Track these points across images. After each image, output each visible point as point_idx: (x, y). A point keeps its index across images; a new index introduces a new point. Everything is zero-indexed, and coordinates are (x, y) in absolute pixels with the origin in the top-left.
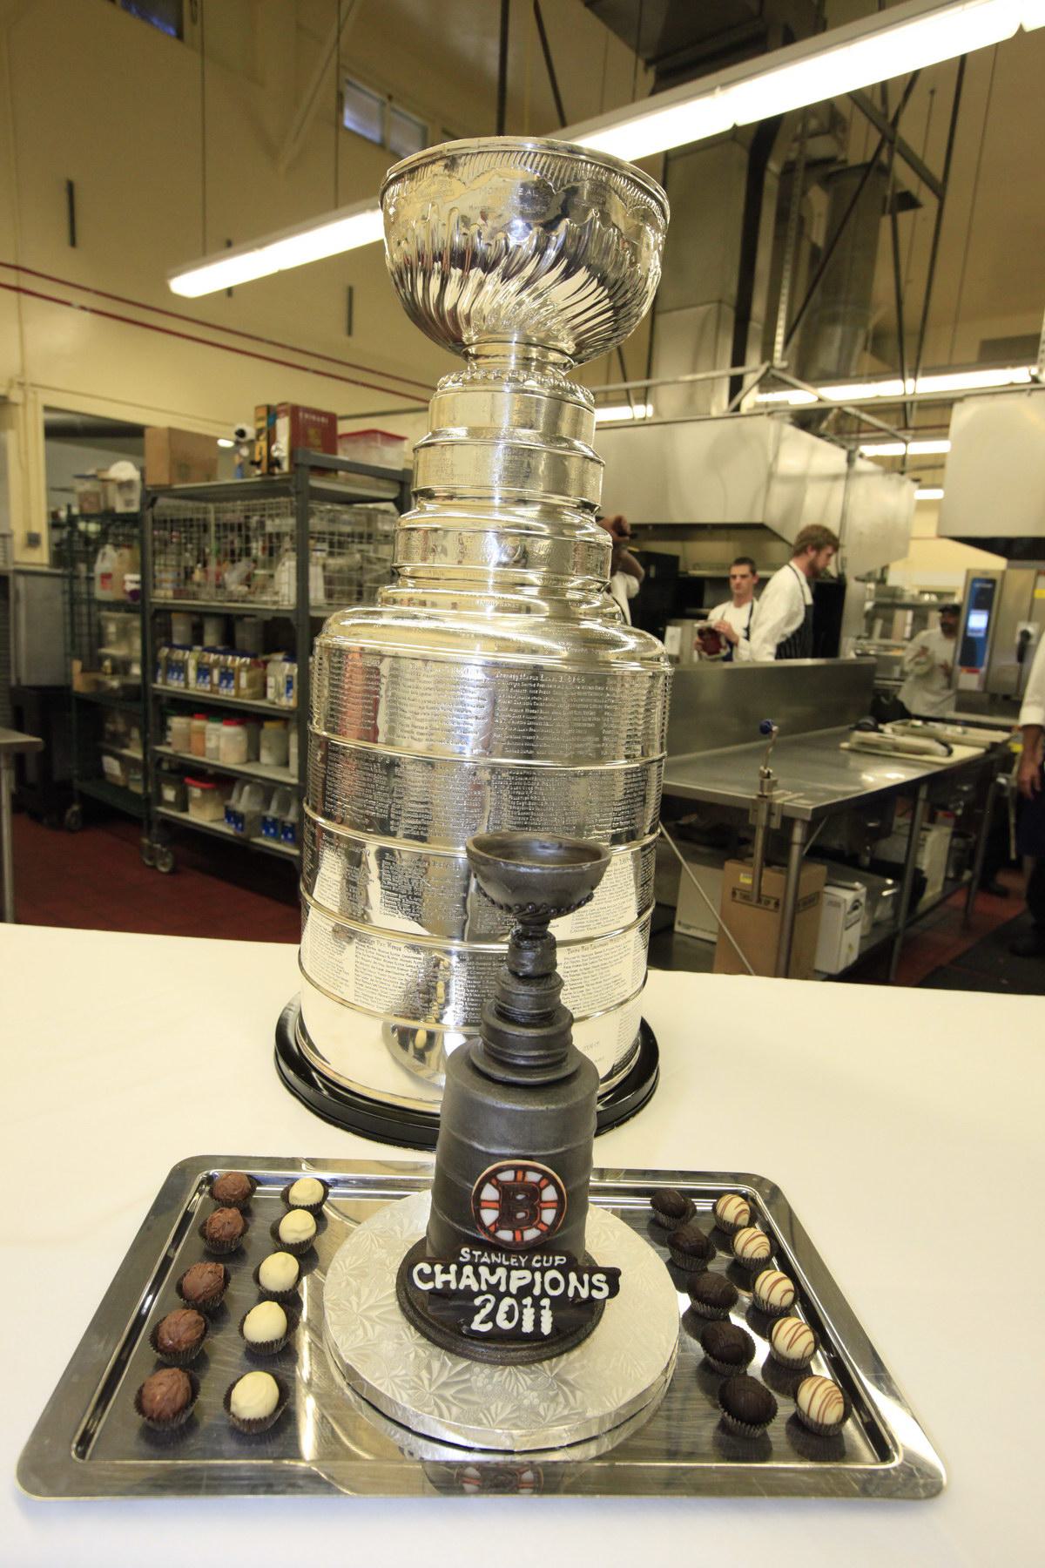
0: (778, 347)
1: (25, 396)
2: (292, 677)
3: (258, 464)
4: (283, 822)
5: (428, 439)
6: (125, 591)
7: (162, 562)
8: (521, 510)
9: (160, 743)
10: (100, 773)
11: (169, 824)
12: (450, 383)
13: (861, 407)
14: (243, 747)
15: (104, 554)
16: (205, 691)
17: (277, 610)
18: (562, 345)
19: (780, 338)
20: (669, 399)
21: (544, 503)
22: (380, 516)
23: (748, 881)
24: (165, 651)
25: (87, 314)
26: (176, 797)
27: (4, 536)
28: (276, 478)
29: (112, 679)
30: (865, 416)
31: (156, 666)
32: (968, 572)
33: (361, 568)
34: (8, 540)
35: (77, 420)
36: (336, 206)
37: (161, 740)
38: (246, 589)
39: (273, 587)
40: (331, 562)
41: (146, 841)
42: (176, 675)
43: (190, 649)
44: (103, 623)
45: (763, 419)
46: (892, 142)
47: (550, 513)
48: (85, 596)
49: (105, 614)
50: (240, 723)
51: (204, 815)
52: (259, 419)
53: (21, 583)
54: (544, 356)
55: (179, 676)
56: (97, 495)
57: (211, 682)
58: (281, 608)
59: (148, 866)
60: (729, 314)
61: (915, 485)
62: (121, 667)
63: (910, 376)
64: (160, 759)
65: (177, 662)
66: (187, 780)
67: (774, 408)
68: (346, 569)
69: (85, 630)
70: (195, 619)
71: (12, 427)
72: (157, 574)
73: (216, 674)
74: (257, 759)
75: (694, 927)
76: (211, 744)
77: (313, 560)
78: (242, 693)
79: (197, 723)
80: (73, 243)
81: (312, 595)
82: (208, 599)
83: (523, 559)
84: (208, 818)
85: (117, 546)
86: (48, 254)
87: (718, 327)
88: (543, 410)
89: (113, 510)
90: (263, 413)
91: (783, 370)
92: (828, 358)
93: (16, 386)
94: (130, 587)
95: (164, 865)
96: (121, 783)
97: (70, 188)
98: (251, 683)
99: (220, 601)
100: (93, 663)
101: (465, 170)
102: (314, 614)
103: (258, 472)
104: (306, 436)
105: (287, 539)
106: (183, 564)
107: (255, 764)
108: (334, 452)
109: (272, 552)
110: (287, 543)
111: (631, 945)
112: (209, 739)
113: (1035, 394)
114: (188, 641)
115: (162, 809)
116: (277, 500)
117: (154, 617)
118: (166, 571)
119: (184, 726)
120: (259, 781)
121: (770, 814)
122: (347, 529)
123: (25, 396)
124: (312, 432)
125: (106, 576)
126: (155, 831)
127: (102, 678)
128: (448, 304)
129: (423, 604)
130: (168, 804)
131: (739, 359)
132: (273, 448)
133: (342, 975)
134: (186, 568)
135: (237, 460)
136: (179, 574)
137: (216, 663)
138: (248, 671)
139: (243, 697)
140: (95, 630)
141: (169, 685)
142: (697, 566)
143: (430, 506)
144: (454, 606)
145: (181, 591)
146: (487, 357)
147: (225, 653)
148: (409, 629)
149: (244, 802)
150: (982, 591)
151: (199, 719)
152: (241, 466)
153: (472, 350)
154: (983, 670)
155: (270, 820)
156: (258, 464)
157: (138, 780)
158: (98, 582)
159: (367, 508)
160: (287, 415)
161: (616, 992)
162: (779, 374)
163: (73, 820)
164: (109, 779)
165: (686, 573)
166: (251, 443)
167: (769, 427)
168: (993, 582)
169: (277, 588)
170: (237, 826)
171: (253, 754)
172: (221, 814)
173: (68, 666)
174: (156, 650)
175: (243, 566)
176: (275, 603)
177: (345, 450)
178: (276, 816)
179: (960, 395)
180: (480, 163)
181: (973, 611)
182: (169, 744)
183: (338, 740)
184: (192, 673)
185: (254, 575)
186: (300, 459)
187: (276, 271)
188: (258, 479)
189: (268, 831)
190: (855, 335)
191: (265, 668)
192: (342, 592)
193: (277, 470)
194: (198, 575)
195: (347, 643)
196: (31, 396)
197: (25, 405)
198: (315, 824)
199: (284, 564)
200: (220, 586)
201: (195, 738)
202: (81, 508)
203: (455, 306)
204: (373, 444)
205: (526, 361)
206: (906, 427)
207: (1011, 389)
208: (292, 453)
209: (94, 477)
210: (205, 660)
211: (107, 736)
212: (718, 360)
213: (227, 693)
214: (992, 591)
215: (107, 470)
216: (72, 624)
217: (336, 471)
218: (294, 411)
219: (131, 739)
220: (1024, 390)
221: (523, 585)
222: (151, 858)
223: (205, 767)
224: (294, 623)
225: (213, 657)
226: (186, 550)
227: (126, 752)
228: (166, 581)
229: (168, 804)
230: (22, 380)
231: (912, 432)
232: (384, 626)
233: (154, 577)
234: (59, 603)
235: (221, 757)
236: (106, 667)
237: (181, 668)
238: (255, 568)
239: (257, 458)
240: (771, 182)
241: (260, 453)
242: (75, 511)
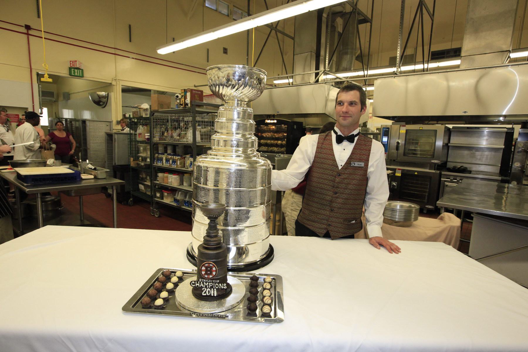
0: (327, 65)
1: (116, 83)
2: (192, 162)
3: (182, 105)
4: (190, 202)
5: (217, 120)
6: (145, 138)
7: (156, 130)
8: (237, 135)
9: (155, 181)
10: (138, 189)
11: (158, 203)
12: (221, 109)
13: (352, 81)
14: (179, 181)
15: (139, 128)
16: (169, 166)
17: (188, 143)
18: (246, 100)
19: (327, 63)
20: (298, 79)
21: (242, 134)
22: (215, 117)
24: (157, 155)
25: (134, 60)
26: (160, 195)
27: (110, 122)
28: (187, 108)
29: (142, 163)
30: (353, 82)
31: (154, 159)
32: (381, 125)
33: (210, 131)
34: (111, 123)
35: (130, 88)
36: (203, 31)
37: (156, 180)
38: (179, 137)
39: (187, 137)
40: (202, 130)
41: (151, 208)
42: (160, 161)
43: (164, 155)
44: (139, 147)
45: (324, 84)
47: (244, 136)
48: (134, 140)
49: (140, 144)
50: (177, 175)
51: (168, 200)
52: (182, 93)
53: (116, 136)
54: (241, 102)
55: (161, 162)
56: (138, 112)
57: (170, 163)
58: (188, 143)
59: (153, 215)
61: (369, 100)
62: (144, 159)
63: (365, 70)
64: (156, 184)
65: (160, 158)
66: (163, 191)
67: (327, 82)
68: (206, 132)
69: (134, 149)
70: (165, 145)
71: (113, 92)
72: (154, 134)
73: (171, 161)
74: (183, 184)
76: (170, 181)
77: (197, 130)
78: (178, 166)
79: (166, 175)
80: (130, 41)
81: (197, 140)
82: (168, 141)
83: (238, 146)
84: (169, 202)
85: (143, 125)
86: (124, 44)
87: (311, 59)
88: (241, 115)
89: (142, 116)
90: (184, 92)
91: (328, 71)
92: (344, 64)
93: (114, 80)
94: (147, 137)
95: (157, 215)
96: (144, 192)
97: (130, 26)
98: (181, 163)
99: (171, 141)
100: (136, 158)
101: (222, 70)
102: (197, 144)
103: (182, 107)
104: (195, 97)
105: (190, 123)
106: (161, 131)
107: (182, 186)
108: (203, 101)
109: (187, 128)
110: (190, 125)
111: (264, 228)
112: (169, 179)
113: (395, 77)
114: (163, 151)
115: (156, 199)
116: (187, 114)
117: (153, 145)
118: (157, 133)
119: (162, 176)
120: (183, 191)
122: (207, 120)
123: (116, 83)
124: (196, 96)
125: (140, 134)
126: (154, 205)
127: (140, 163)
128: (220, 92)
129: (217, 155)
130: (158, 198)
131: (317, 68)
132: (186, 101)
133: (201, 235)
134: (162, 132)
135: (176, 103)
136: (160, 134)
137: (171, 158)
138: (179, 160)
139: (178, 168)
140: (137, 149)
141: (158, 164)
142: (308, 125)
143: (218, 134)
144: (224, 156)
145: (161, 138)
146: (229, 103)
147: (173, 155)
148: (213, 161)
149: (179, 197)
150: (386, 131)
151: (166, 173)
152: (177, 105)
153: (227, 101)
155: (186, 201)
156: (182, 105)
157: (149, 191)
158: (138, 135)
159: (213, 115)
160: (189, 91)
161: (262, 237)
162: (327, 72)
163: (131, 203)
164: (140, 190)
165: (305, 127)
166: (180, 99)
167: (326, 86)
168: (388, 128)
169: (187, 137)
170: (177, 203)
171: (182, 183)
172: (173, 200)
173: (129, 160)
174: (154, 155)
175: (178, 131)
176: (187, 141)
177: (205, 100)
178: (188, 200)
180: (225, 69)
181: (383, 137)
182: (158, 181)
183: (199, 185)
184: (164, 161)
185: (181, 133)
186: (193, 104)
187: (186, 47)
188: (182, 108)
189: (186, 204)
190: (352, 57)
191: (185, 159)
192: (205, 138)
193: (187, 106)
194: (166, 134)
195: (201, 164)
196: (118, 83)
197: (116, 85)
198: (194, 203)
199: (189, 131)
200: (172, 137)
201: (165, 179)
202: (133, 115)
203: (222, 93)
204: (213, 98)
205: (238, 104)
206: (366, 85)
208: (191, 102)
209: (137, 107)
210: (168, 157)
211: (140, 179)
212: (312, 68)
213: (174, 166)
215: (141, 106)
216: (130, 149)
217: (203, 106)
218: (191, 91)
219: (147, 179)
220: (393, 76)
221: (238, 151)
222: (153, 213)
223: (168, 187)
224: (192, 147)
225: (170, 156)
226: (162, 127)
227: (145, 183)
228: (157, 136)
229: (158, 198)
230: (116, 79)
231: (367, 86)
232: (208, 161)
233: (154, 134)
234: (127, 142)
235: (173, 184)
236: (140, 159)
237: (161, 159)
238: (181, 132)
239: (182, 103)
240: (324, 19)
241: (182, 102)
242: (131, 116)
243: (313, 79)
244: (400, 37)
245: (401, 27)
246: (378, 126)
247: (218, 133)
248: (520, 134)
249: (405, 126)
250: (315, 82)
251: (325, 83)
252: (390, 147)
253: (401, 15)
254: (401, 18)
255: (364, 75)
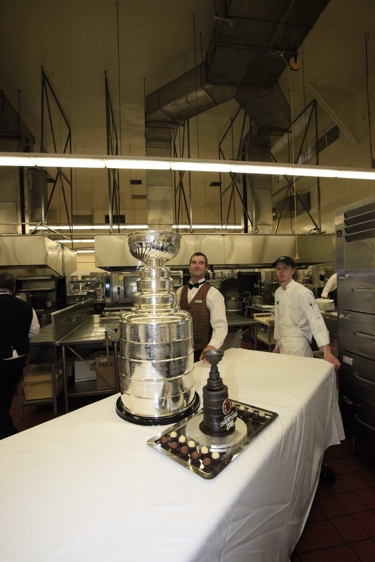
0: (43, 218)
8: (165, 292)
19: (43, 216)
23: (105, 360)
30: (64, 236)
46: (60, 172)
47: (169, 293)
60: (19, 205)
75: (81, 379)
87: (17, 210)
121: (109, 342)
142: (19, 277)
154: (111, 297)
168: (109, 277)
179: (95, 234)
181: (106, 284)
207: (93, 229)
214: (110, 278)
240: (25, 172)
243: (20, 229)
244: (110, 204)
245: (110, 196)
246: (82, 274)
247: (145, 291)
248: (184, 276)
249: (122, 274)
250: (32, 234)
251: (43, 235)
252: (113, 292)
253: (109, 188)
254: (109, 190)
255: (70, 229)
